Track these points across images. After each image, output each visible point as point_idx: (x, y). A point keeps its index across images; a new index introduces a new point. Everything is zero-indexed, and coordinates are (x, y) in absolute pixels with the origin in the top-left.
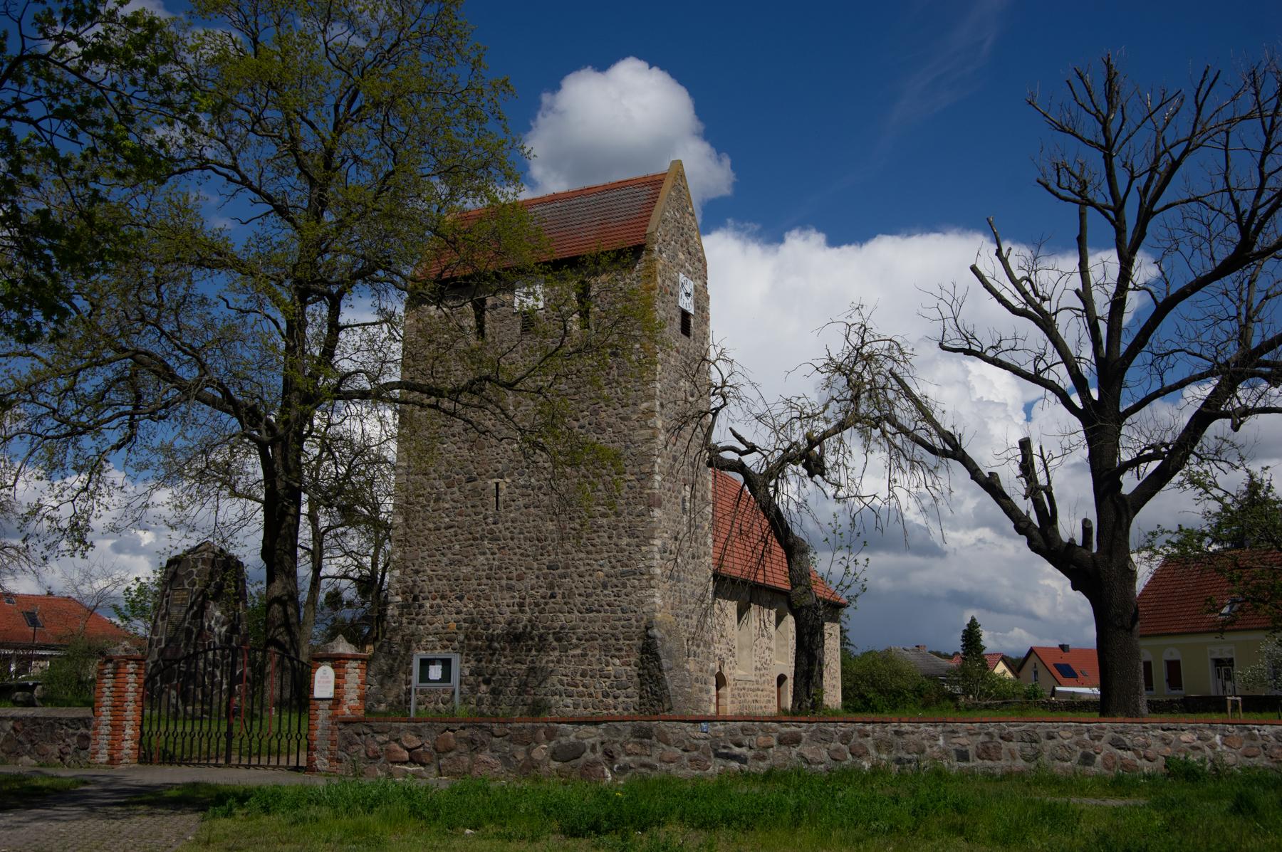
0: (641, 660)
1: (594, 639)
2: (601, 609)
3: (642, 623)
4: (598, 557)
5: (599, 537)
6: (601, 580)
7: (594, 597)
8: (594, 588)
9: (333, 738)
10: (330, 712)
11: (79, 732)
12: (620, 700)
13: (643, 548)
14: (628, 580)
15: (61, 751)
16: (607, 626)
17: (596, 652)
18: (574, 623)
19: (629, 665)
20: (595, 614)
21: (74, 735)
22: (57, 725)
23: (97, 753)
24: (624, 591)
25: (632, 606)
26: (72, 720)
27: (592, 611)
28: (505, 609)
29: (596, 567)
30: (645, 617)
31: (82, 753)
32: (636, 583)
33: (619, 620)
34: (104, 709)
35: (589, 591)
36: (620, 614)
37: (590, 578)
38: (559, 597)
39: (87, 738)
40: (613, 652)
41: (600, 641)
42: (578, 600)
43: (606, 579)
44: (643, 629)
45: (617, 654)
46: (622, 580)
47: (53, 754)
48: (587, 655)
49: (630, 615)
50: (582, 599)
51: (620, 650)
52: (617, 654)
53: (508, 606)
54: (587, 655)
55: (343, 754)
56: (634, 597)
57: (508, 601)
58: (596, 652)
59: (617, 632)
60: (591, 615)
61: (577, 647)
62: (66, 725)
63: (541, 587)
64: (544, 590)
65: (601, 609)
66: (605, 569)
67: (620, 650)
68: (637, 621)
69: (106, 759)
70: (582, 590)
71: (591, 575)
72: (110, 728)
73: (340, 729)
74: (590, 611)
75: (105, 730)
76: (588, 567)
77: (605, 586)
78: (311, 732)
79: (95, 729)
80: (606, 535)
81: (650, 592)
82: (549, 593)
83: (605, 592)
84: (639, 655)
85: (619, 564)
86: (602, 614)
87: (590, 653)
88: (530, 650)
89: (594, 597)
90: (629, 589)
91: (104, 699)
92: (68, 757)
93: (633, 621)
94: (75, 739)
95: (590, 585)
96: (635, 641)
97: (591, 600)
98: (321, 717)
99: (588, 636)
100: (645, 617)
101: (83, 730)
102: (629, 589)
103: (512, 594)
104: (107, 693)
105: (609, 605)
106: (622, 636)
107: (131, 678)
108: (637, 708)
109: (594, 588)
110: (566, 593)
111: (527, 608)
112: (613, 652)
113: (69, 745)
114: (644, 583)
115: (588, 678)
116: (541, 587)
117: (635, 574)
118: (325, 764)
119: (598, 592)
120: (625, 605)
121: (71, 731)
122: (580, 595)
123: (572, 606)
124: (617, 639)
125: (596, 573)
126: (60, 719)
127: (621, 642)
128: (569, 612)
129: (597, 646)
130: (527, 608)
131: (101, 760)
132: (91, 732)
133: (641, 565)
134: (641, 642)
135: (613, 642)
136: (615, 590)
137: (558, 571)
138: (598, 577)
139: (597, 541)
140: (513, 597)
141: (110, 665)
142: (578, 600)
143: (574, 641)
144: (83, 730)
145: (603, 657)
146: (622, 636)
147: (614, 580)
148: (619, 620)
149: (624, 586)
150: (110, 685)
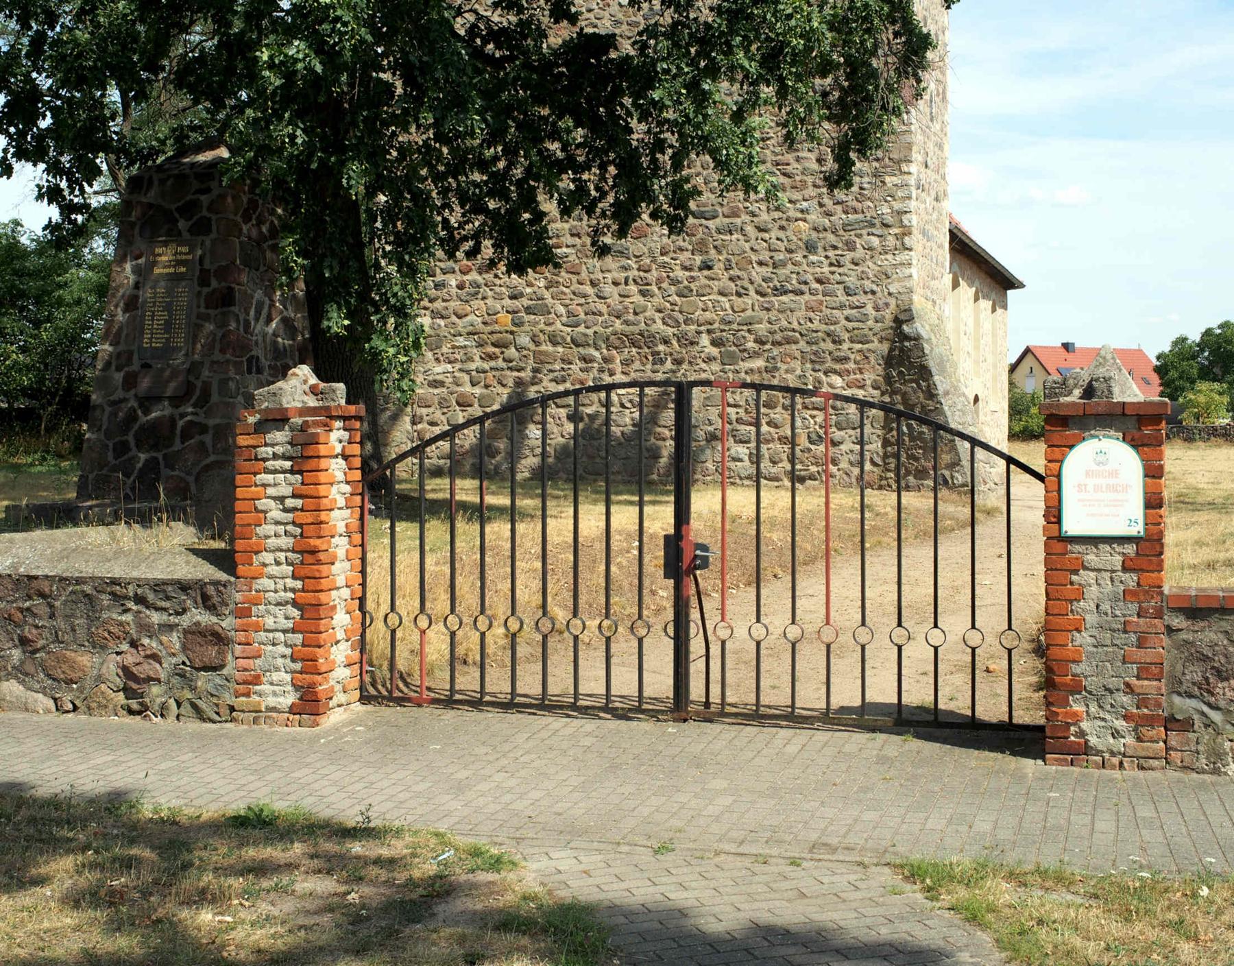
0: (888, 379)
1: (789, 341)
2: (804, 288)
3: (888, 315)
4: (796, 196)
5: (798, 159)
6: (804, 237)
7: (790, 266)
8: (790, 251)
9: (1146, 656)
10: (1131, 580)
11: (185, 621)
12: (843, 447)
13: (888, 179)
14: (859, 236)
15: (127, 672)
16: (816, 317)
17: (796, 364)
18: (749, 313)
19: (862, 387)
20: (791, 296)
21: (171, 627)
22: (105, 599)
23: (256, 680)
24: (849, 256)
25: (867, 283)
26: (159, 586)
27: (786, 292)
28: (608, 289)
29: (793, 214)
30: (893, 302)
31: (203, 681)
32: (875, 241)
33: (841, 307)
34: (268, 557)
35: (780, 256)
36: (842, 297)
37: (781, 234)
38: (718, 268)
39: (219, 639)
40: (829, 364)
41: (802, 344)
42: (758, 273)
43: (814, 235)
44: (889, 322)
45: (838, 367)
46: (846, 236)
47: (99, 679)
48: (776, 369)
49: (863, 298)
50: (766, 271)
51: (845, 359)
52: (838, 367)
53: (616, 284)
54: (776, 369)
55: (1193, 703)
56: (870, 268)
57: (616, 275)
58: (796, 364)
59: (837, 328)
60: (784, 298)
61: (757, 354)
62: (140, 600)
63: (681, 249)
64: (688, 254)
65: (804, 288)
66: (812, 217)
67: (845, 359)
68: (877, 309)
69: (290, 699)
70: (765, 256)
71: (782, 228)
72: (295, 613)
73: (1170, 630)
74: (780, 291)
75: (278, 618)
76: (776, 215)
77: (810, 248)
78: (1059, 638)
79: (244, 613)
80: (813, 156)
81: (903, 257)
82: (698, 259)
83: (813, 258)
84: (880, 370)
85: (839, 208)
86: (807, 297)
87: (783, 367)
88: (662, 362)
89: (790, 266)
90: (860, 253)
91: (268, 529)
92: (155, 690)
93: (869, 310)
94: (175, 640)
95: (781, 246)
96: (875, 345)
97: (783, 272)
98: (1093, 592)
99: (778, 337)
100: (893, 302)
101: (203, 618)
102: (860, 253)
103: (625, 262)
104: (276, 513)
105: (819, 281)
106: (846, 336)
107: (337, 468)
108: (879, 461)
109: (790, 251)
110: (734, 260)
111: (654, 288)
112: (829, 364)
113: (155, 657)
114: (891, 242)
115: (779, 409)
116: (681, 249)
117: (873, 225)
118: (1116, 734)
119: (798, 257)
120: (851, 281)
121: (156, 618)
122: (761, 263)
123: (746, 284)
124: (837, 342)
125: (792, 226)
126: (114, 582)
127: (845, 346)
128: (739, 295)
129: (798, 354)
130: (654, 288)
131: (271, 701)
132: (228, 623)
133: (886, 210)
134: (885, 348)
135: (829, 346)
136: (831, 253)
137: (717, 221)
138: (797, 232)
139: (794, 167)
140: (625, 268)
141: (280, 436)
142: (758, 273)
143: (750, 345)
144: (203, 618)
145: (809, 373)
146: (846, 336)
147: (831, 238)
148: (841, 307)
149: (850, 246)
150: (286, 490)
